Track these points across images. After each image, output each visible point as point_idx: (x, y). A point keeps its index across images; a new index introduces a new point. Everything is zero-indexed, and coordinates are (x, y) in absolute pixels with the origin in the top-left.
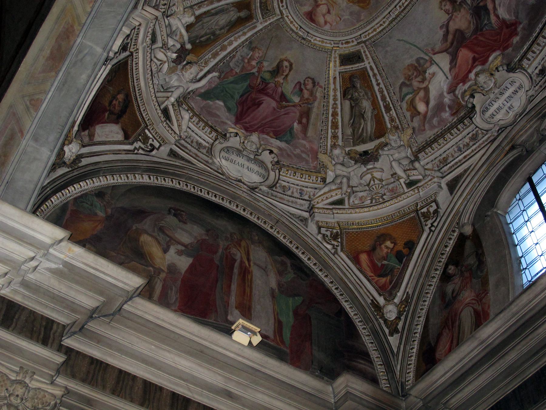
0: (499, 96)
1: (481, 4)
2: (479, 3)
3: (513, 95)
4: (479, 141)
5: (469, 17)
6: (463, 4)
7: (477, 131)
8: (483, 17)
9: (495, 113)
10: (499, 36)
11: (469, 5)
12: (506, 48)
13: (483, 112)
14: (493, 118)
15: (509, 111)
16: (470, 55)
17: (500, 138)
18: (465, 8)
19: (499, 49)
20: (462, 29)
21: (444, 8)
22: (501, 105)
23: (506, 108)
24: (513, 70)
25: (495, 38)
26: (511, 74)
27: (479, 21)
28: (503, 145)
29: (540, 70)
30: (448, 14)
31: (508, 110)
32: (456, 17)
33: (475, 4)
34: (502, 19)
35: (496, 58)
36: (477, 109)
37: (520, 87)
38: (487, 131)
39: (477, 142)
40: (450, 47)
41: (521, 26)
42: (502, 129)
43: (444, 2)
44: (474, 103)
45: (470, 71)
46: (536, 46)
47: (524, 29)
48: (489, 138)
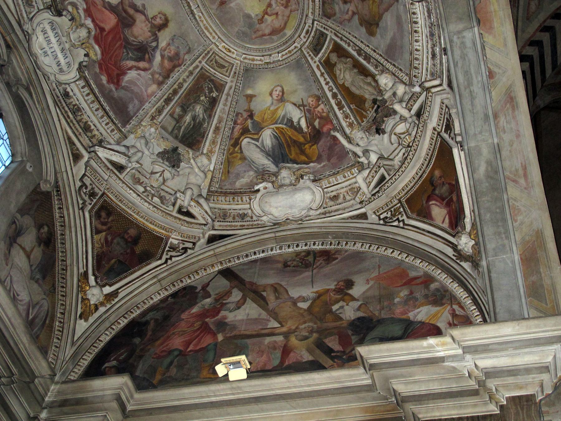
0: (61, 47)
1: (147, 56)
2: (148, 54)
3: (56, 60)
4: (24, 6)
5: (141, 39)
7: (34, 7)
8: (136, 53)
9: (46, 35)
11: (150, 43)
12: (101, 68)
13: (51, 23)
14: (42, 31)
15: (43, 51)
16: (107, 27)
17: (19, 33)
18: (150, 37)
19: (102, 59)
21: (159, 16)
22: (51, 45)
23: (47, 49)
24: (80, 69)
25: (113, 59)
26: (77, 66)
27: (133, 47)
28: (13, 35)
29: (68, 93)
30: (152, 18)
31: (45, 50)
32: (146, 25)
33: (149, 49)
34: (127, 73)
35: (96, 55)
36: (57, 19)
37: (61, 71)
38: (31, 19)
39: (23, 3)
40: (123, 8)
41: (114, 89)
42: (28, 37)
44: (64, 17)
45: (93, 21)
46: (93, 99)
47: (111, 91)
48: (23, 18)
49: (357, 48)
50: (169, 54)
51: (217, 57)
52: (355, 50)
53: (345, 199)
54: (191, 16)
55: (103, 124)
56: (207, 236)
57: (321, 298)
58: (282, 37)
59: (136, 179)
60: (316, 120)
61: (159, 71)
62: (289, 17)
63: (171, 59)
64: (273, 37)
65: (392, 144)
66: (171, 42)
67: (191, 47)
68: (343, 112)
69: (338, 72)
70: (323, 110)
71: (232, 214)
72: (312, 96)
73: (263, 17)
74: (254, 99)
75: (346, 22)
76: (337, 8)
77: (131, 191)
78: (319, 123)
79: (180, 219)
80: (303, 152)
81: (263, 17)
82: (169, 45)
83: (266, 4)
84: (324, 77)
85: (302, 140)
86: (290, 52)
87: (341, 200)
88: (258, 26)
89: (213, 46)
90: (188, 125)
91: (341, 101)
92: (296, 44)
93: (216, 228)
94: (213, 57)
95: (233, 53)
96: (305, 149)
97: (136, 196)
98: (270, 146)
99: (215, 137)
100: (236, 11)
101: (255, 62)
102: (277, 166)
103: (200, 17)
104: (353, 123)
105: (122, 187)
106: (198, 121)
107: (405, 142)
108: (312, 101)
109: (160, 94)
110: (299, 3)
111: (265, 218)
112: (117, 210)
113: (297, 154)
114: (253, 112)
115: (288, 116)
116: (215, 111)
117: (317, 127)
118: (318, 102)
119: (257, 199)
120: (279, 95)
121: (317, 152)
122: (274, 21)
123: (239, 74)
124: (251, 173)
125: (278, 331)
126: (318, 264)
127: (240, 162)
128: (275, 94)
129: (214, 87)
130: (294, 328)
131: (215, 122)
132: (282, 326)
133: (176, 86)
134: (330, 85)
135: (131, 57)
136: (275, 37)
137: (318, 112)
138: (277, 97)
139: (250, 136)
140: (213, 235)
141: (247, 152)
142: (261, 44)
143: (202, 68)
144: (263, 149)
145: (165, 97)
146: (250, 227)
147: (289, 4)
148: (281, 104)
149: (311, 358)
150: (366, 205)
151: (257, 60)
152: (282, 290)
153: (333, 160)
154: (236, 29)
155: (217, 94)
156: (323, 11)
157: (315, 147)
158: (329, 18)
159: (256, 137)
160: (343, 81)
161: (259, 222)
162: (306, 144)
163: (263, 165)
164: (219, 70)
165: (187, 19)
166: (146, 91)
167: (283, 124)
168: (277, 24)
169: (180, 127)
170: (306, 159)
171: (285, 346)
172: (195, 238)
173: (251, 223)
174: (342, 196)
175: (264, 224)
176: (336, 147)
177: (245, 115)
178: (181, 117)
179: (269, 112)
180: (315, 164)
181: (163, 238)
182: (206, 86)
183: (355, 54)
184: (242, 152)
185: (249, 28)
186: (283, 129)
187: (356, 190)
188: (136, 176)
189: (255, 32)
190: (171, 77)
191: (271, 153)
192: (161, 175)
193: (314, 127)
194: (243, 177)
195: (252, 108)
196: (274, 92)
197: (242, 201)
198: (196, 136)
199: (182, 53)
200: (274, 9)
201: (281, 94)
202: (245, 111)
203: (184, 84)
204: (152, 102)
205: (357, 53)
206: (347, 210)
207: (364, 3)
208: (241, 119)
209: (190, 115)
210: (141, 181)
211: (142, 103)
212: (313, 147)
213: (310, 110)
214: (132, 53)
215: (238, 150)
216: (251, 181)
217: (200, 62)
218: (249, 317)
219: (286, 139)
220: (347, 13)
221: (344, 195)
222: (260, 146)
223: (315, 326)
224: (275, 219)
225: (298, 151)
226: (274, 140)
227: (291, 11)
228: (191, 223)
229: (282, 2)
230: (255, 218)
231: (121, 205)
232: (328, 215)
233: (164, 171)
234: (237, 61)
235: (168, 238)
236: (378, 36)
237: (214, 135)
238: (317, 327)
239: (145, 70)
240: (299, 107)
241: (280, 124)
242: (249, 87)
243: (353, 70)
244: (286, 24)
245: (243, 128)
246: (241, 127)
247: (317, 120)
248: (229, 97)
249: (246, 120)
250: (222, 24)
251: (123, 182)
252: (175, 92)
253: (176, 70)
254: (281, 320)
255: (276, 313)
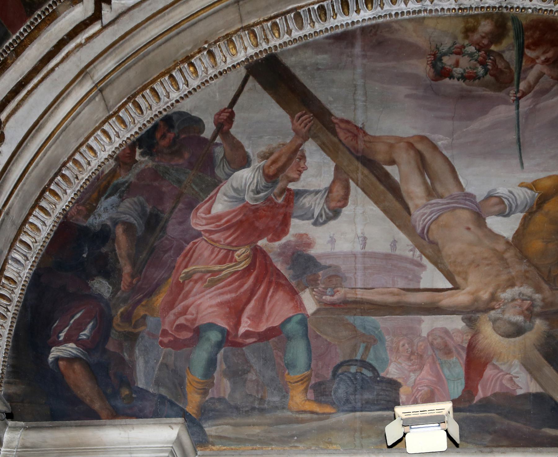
57: (548, 206)
125: (447, 301)
126: (531, 76)
130: (485, 296)
132: (456, 287)
149: (534, 388)
152: (437, 165)
171: (471, 348)
218: (368, 249)
223: (537, 296)
238: (543, 300)
254: (451, 269)
255: (433, 243)
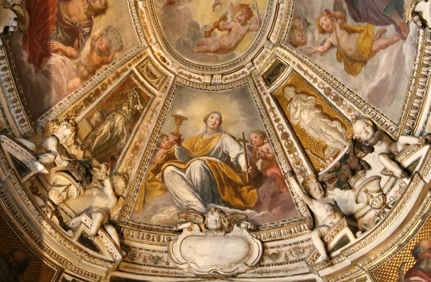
1: (76, 42)
5: (74, 19)
6: (89, 21)
8: (66, 35)
10: (40, 39)
11: (84, 27)
12: (25, 41)
20: (70, 3)
27: (65, 27)
32: (84, 5)
33: (81, 34)
41: (33, 71)
43: (103, 3)
47: (30, 71)
49: (327, 85)
50: (100, 47)
51: (150, 64)
52: (322, 88)
53: (288, 259)
54: (133, 8)
55: (13, 111)
56: (109, 277)
58: (229, 58)
59: (33, 189)
60: (258, 159)
61: (84, 62)
62: (243, 36)
63: (101, 53)
64: (219, 56)
65: (357, 202)
66: (105, 33)
67: (124, 44)
68: (294, 156)
69: (293, 110)
70: (268, 149)
71: (142, 255)
72: (256, 132)
73: (212, 30)
74: (184, 122)
75: (318, 55)
76: (309, 37)
77: (30, 202)
78: (262, 164)
79: (81, 250)
80: (239, 195)
81: (212, 30)
82: (101, 35)
83: (221, 15)
84: (273, 112)
85: (238, 180)
86: (236, 76)
87: (282, 259)
88: (204, 39)
89: (149, 50)
90: (104, 135)
91: (292, 143)
92: (245, 69)
93: (121, 269)
94: (145, 63)
95: (168, 64)
96: (242, 191)
97: (34, 209)
98: (199, 180)
99: (133, 157)
100: (183, 16)
101: (192, 80)
102: (205, 206)
103: (142, 13)
104: (306, 171)
105: (20, 195)
106: (115, 134)
107: (376, 201)
108: (256, 138)
109: (81, 91)
110: (260, 23)
111: (184, 266)
112: (6, 223)
113: (231, 195)
114: (182, 138)
115: (224, 149)
116: (136, 126)
117: (259, 168)
118: (263, 140)
119: (179, 242)
120: (215, 123)
121: (256, 197)
122: (224, 38)
123: (171, 90)
124: (173, 209)
127: (160, 193)
128: (211, 121)
129: (140, 98)
131: (136, 139)
133: (99, 87)
134: (280, 123)
135: (60, 37)
136: (220, 56)
137: (262, 151)
138: (213, 125)
139: (174, 164)
140: (116, 277)
141: (169, 183)
142: (202, 61)
143: (130, 74)
144: (189, 183)
145: (86, 96)
146: (165, 274)
147: (249, 22)
148: (217, 134)
150: (320, 269)
151: (194, 78)
153: (275, 211)
154: (178, 37)
155: (142, 107)
156: (290, 38)
157: (254, 191)
158: (295, 46)
159: (182, 166)
160: (298, 121)
161: (178, 271)
162: (244, 186)
163: (189, 202)
164: (149, 79)
165: (128, 11)
166: (67, 83)
167: (216, 158)
168: (227, 41)
169: (95, 137)
170: (242, 204)
172: (95, 277)
173: (166, 270)
174: (283, 255)
175: (183, 274)
176: (281, 196)
177: (172, 139)
178: (99, 124)
179: (201, 140)
180: (253, 211)
181: (54, 271)
182: (132, 95)
183: (322, 91)
184: (163, 181)
185: (192, 39)
186: (216, 163)
187: (302, 250)
188: (35, 185)
189: (198, 46)
190: (96, 74)
191: (199, 189)
192: (65, 190)
193: (255, 168)
194: (161, 212)
195: (181, 132)
196: (210, 119)
197: (159, 241)
198: (110, 151)
199: (113, 49)
200: (228, 24)
201: (217, 122)
202: (172, 133)
203: (108, 86)
204: (72, 98)
205: (325, 91)
206: (289, 273)
207: (352, 35)
208: (167, 142)
209: (108, 124)
210: (39, 193)
211: (60, 96)
212: (252, 191)
213: (253, 148)
214: (62, 33)
215: (159, 178)
216: (171, 219)
217: (130, 65)
219: (219, 176)
220: (322, 44)
221: (286, 254)
222: (187, 179)
224: (199, 269)
225: (233, 193)
226: (204, 174)
227: (248, 30)
228: (94, 257)
229: (240, 17)
230: (171, 264)
231: (12, 217)
232: (265, 275)
233: (70, 185)
234: (170, 74)
235: (62, 271)
236: (362, 76)
237: (132, 155)
239: (71, 57)
240: (238, 141)
241: (213, 156)
242: (180, 107)
243: (314, 110)
244: (237, 44)
245: (167, 153)
246: (165, 151)
247: (260, 161)
248: (155, 114)
249: (172, 144)
250: (164, 27)
251: (24, 189)
252: (97, 93)
253: (104, 67)
